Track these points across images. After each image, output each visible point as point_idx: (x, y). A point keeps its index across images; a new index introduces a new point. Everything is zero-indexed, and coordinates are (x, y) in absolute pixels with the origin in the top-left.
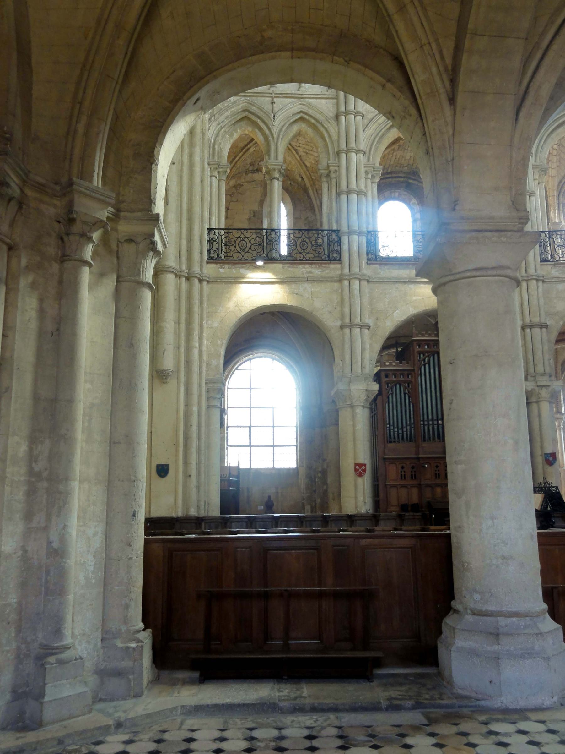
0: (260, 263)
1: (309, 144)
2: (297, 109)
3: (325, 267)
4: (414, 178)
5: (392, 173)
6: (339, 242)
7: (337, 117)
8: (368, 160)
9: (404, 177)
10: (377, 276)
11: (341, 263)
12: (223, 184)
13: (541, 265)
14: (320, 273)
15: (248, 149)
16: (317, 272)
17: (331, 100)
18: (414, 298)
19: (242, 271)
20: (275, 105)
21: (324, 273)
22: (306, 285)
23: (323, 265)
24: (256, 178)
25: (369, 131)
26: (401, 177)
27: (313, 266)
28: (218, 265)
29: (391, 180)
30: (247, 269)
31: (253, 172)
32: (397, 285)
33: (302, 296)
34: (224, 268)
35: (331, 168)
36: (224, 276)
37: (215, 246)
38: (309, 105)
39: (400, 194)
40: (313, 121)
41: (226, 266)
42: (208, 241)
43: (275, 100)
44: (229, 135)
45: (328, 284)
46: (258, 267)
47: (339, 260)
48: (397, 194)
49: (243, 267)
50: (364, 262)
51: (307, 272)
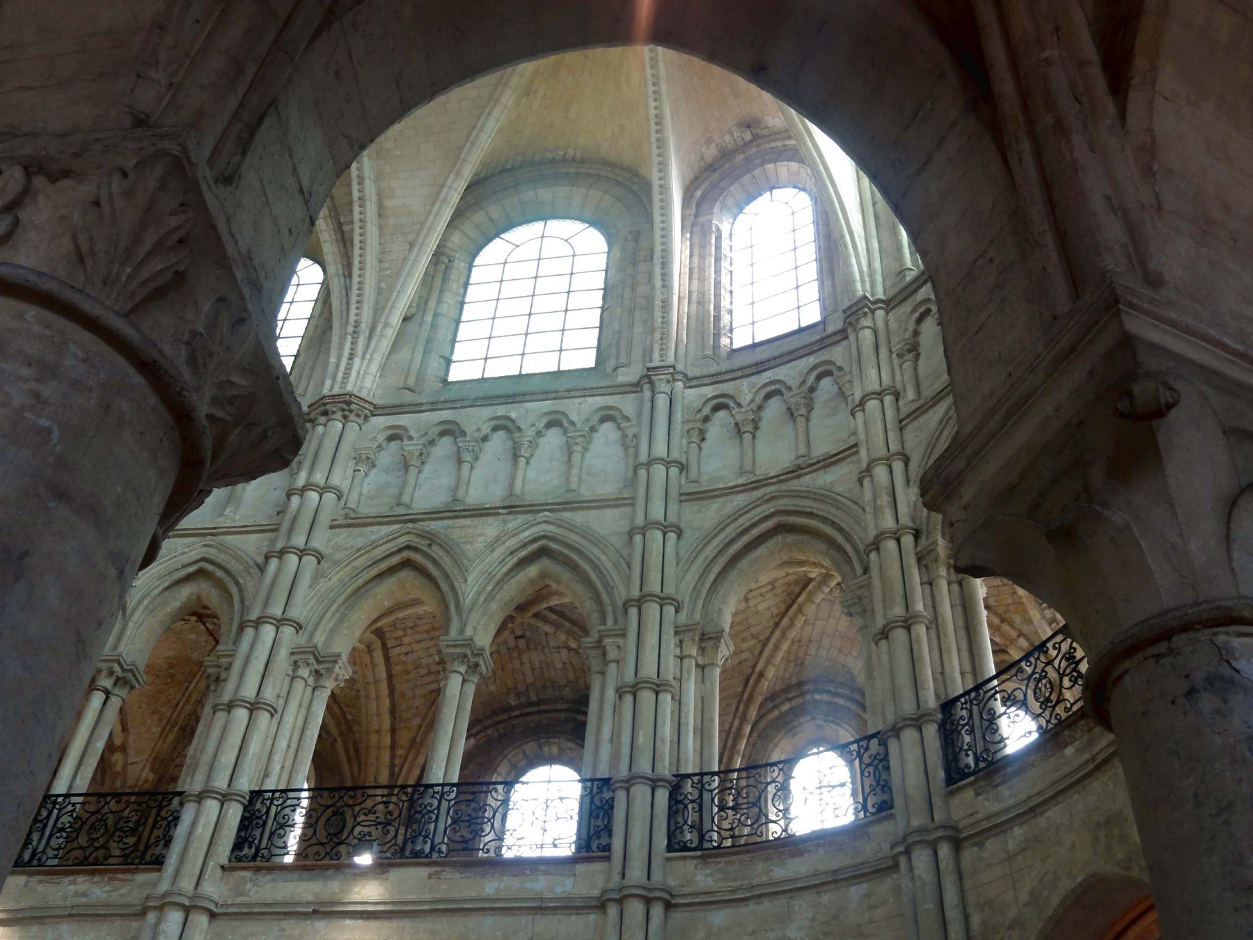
2: (194, 555)
3: (122, 880)
5: (538, 703)
10: (238, 900)
13: (668, 859)
14: (105, 895)
16: (98, 892)
21: (115, 894)
23: (120, 876)
25: (323, 586)
26: (561, 711)
29: (536, 717)
32: (284, 923)
38: (221, 548)
39: (560, 749)
40: (219, 573)
45: (118, 923)
48: (555, 750)
51: (77, 894)
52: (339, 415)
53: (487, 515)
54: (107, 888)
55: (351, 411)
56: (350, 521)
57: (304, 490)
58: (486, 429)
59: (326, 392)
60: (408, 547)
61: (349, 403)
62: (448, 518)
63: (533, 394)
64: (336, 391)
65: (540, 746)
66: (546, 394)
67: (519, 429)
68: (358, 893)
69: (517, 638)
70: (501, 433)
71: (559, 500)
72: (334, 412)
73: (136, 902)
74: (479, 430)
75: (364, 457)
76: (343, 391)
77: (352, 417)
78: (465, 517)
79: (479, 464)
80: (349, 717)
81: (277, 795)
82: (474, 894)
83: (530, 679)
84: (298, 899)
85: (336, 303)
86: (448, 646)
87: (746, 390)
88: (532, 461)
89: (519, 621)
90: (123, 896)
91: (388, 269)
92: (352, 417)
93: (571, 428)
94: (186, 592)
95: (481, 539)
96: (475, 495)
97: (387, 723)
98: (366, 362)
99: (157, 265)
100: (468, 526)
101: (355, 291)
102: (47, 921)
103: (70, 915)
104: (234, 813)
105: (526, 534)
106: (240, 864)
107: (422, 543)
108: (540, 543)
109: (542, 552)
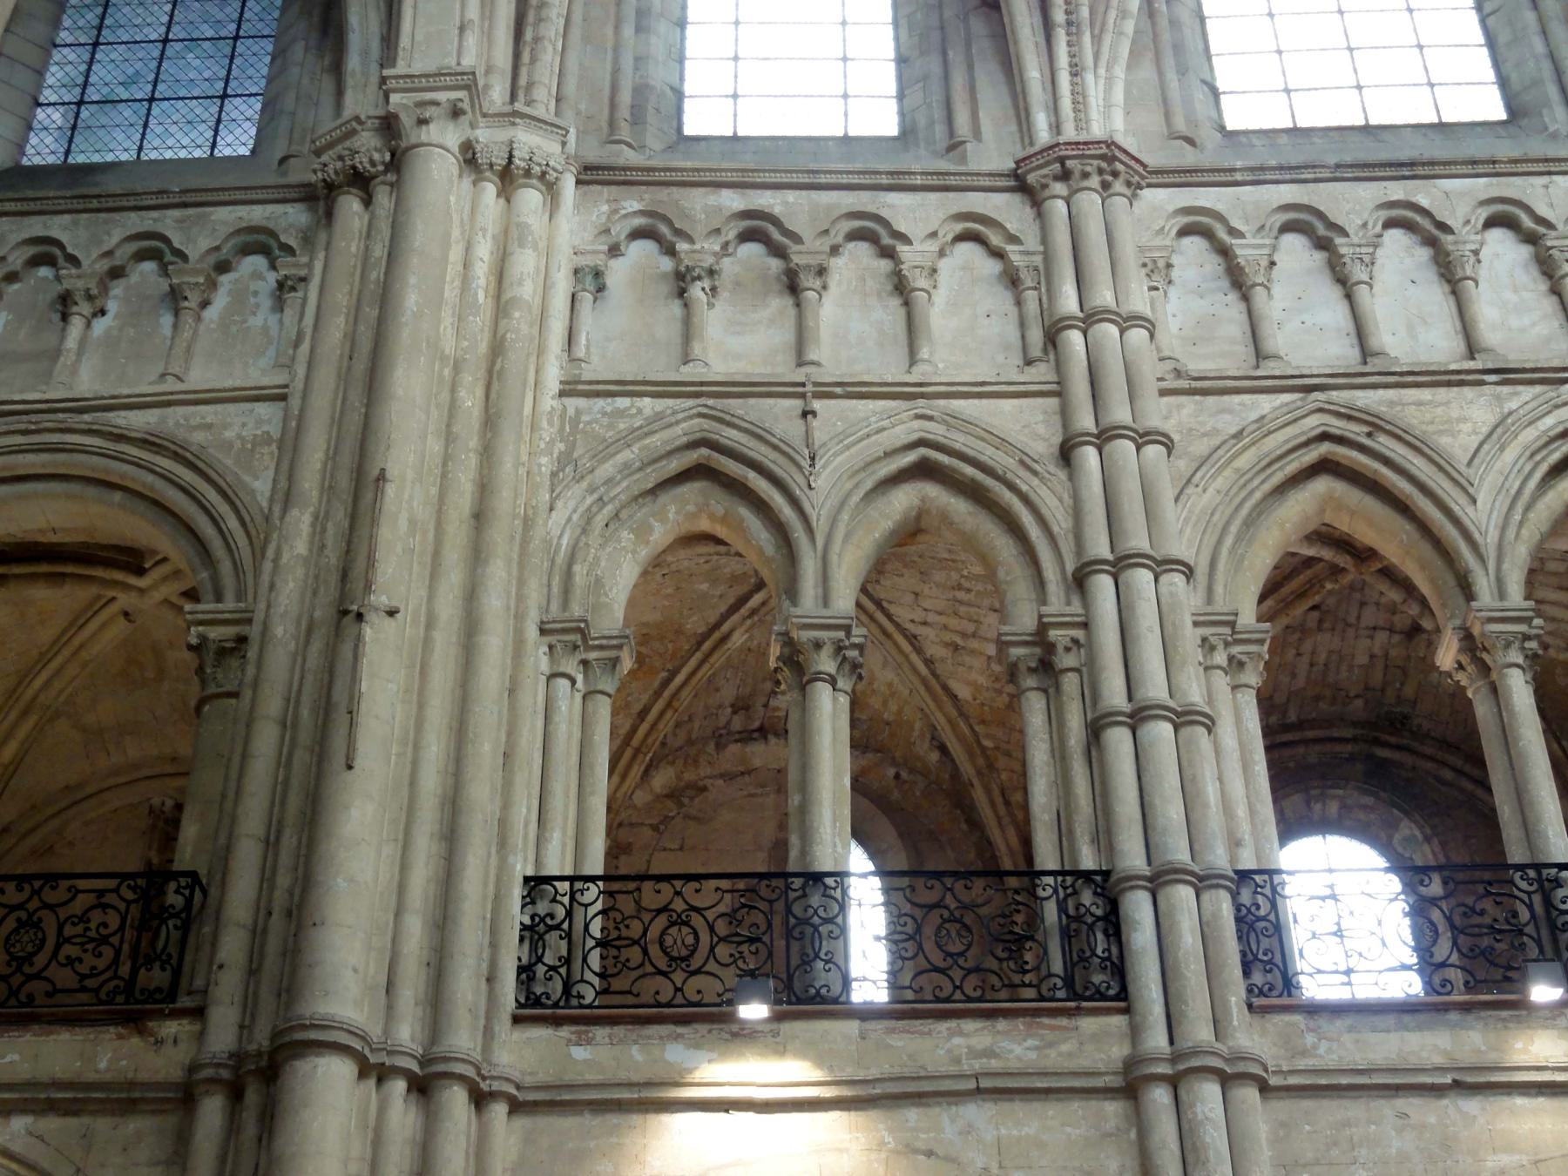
0: (754, 1011)
1: (963, 609)
3: (1053, 1028)
4: (1393, 740)
5: (1300, 725)
6: (1114, 923)
7: (1066, 454)
8: (1210, 599)
9: (1354, 740)
10: (1302, 1064)
11: (1127, 1011)
12: (603, 710)
14: (1033, 1055)
15: (725, 638)
16: (1018, 1050)
17: (1040, 400)
18: (1494, 1161)
19: (675, 1053)
20: (815, 423)
21: (1053, 1053)
22: (973, 1112)
23: (1046, 1021)
24: (757, 762)
27: (1002, 1024)
28: (565, 1032)
29: (1301, 750)
30: (697, 1046)
31: (746, 737)
32: (1401, 1103)
33: (952, 1160)
34: (589, 1042)
35: (1053, 634)
37: (555, 947)
39: (1344, 806)
41: (601, 1033)
42: (524, 927)
43: (817, 405)
44: (632, 530)
45: (1076, 1106)
46: (744, 1036)
47: (1121, 997)
48: (1333, 808)
49: (679, 1037)
50: (1236, 997)
51: (975, 1054)
52: (1095, 181)
53: (1461, 383)
54: (1030, 1042)
55: (1115, 174)
59: (1043, 136)
60: (1325, 437)
62: (1386, 386)
63: (1432, 163)
65: (1308, 803)
67: (1443, 227)
68: (1526, 1051)
72: (1086, 175)
73: (1102, 1067)
74: (1365, 225)
75: (1161, 264)
76: (1083, 137)
77: (1118, 186)
80: (987, 743)
84: (1413, 1061)
86: (1491, 620)
90: (1070, 1055)
94: (904, 499)
95: (1466, 427)
102: (931, 1101)
103: (979, 1091)
105: (1549, 421)
107: (1355, 431)
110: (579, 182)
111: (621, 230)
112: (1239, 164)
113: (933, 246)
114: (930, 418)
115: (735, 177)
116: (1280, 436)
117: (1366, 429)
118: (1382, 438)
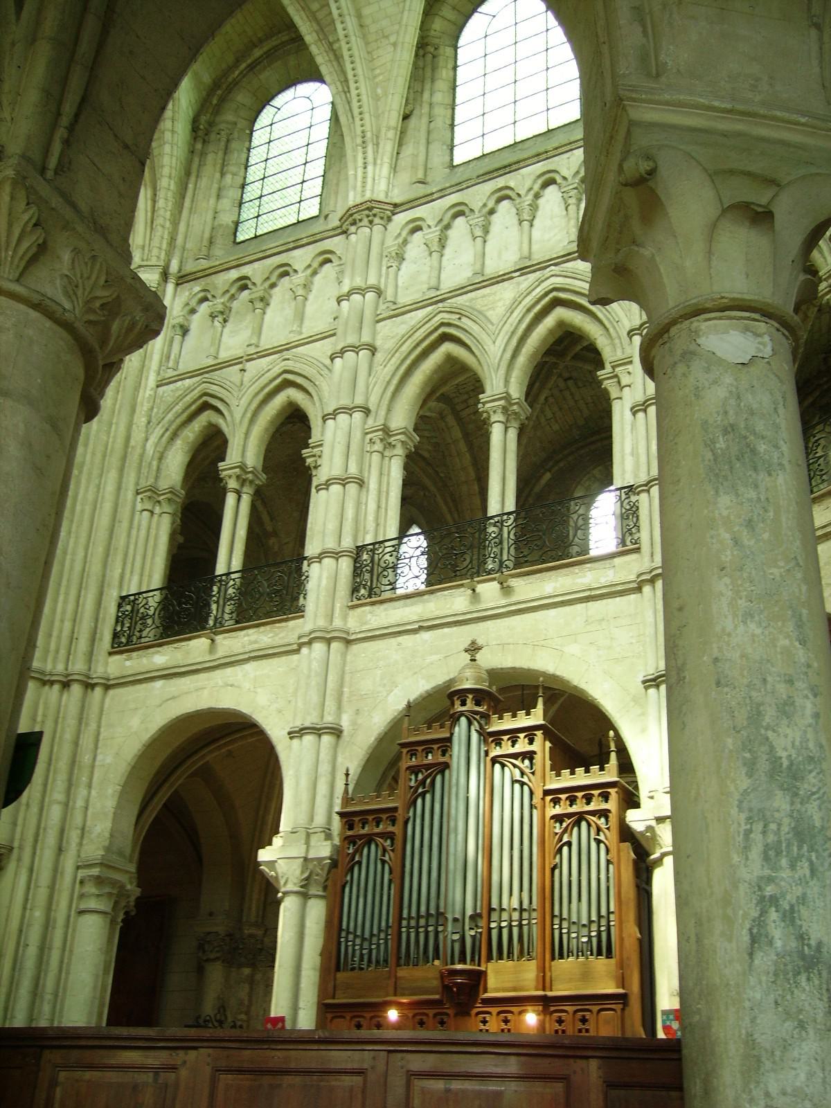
14: (270, 640)
16: (265, 639)
21: (277, 638)
28: (124, 656)
32: (400, 639)
36: (130, 672)
41: (134, 654)
43: (249, 365)
49: (159, 652)
51: (251, 643)
52: (365, 222)
53: (503, 281)
56: (392, 313)
57: (349, 294)
58: (491, 204)
59: (351, 203)
60: (442, 324)
61: (370, 209)
62: (471, 291)
64: (359, 201)
66: (539, 157)
67: (519, 195)
69: (566, 380)
70: (505, 203)
71: (562, 254)
72: (360, 220)
77: (377, 220)
78: (484, 287)
79: (489, 237)
80: (442, 475)
81: (377, 546)
82: (536, 595)
83: (586, 413)
84: (406, 620)
85: (343, 119)
87: (478, 196)
88: (535, 222)
89: (561, 366)
90: (283, 638)
91: (379, 74)
92: (377, 220)
93: (564, 183)
95: (500, 304)
96: (494, 266)
97: (473, 475)
98: (378, 167)
99: (25, 245)
100: (489, 295)
101: (355, 104)
104: (346, 565)
106: (360, 602)
107: (453, 318)
108: (551, 296)
109: (557, 302)
110: (178, 284)
111: (193, 303)
112: (434, 190)
113: (309, 271)
114: (288, 359)
115: (235, 263)
116: (422, 330)
117: (458, 316)
118: (464, 319)
